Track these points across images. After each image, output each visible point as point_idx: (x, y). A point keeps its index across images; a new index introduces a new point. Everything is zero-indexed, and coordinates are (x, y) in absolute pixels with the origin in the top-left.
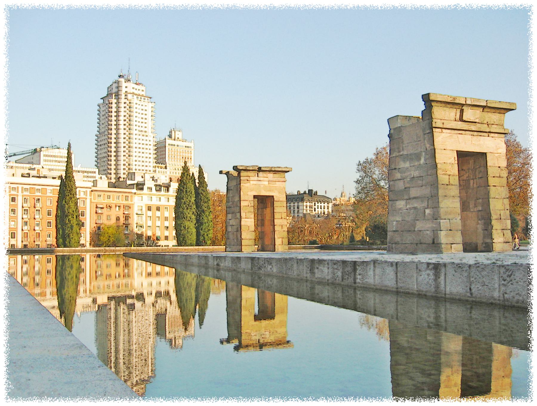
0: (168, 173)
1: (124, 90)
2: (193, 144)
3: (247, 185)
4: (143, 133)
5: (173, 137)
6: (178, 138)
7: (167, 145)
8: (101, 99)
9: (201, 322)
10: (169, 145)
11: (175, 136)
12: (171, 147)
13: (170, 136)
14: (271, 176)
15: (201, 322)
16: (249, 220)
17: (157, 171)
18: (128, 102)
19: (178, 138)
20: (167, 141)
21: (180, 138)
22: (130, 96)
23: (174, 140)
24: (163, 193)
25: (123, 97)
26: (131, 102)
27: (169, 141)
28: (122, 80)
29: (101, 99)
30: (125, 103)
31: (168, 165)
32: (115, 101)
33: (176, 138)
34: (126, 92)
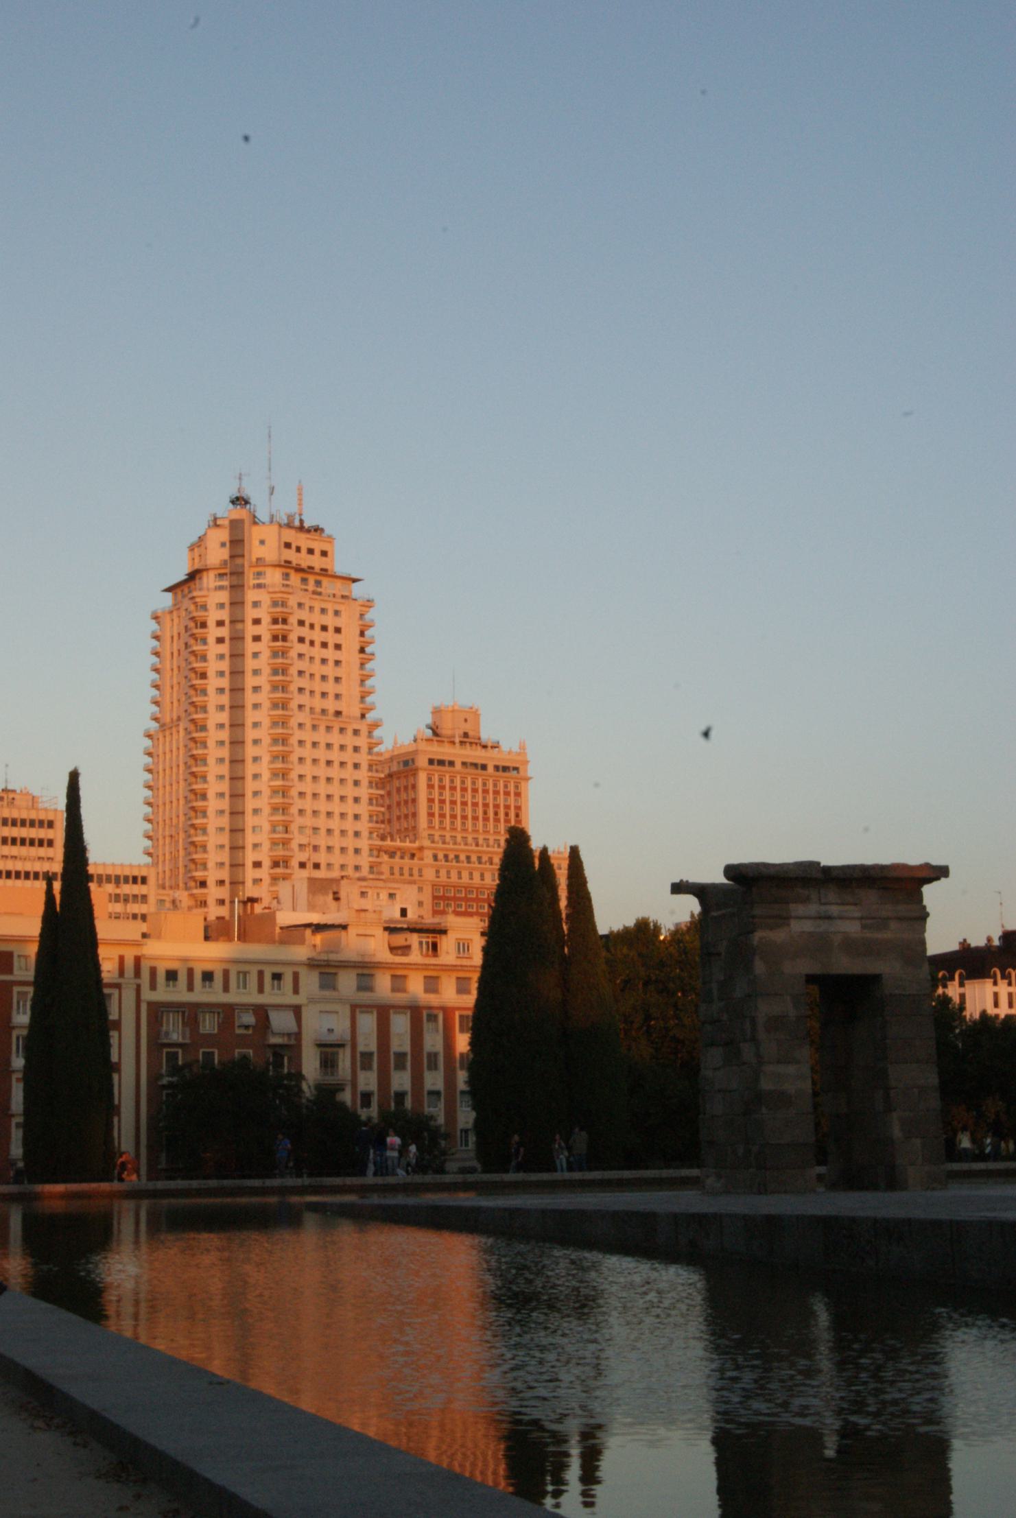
0: (429, 874)
3: (779, 936)
5: (446, 730)
6: (466, 735)
7: (422, 762)
10: (431, 762)
14: (870, 897)
16: (791, 1069)
17: (385, 869)
30: (256, 604)
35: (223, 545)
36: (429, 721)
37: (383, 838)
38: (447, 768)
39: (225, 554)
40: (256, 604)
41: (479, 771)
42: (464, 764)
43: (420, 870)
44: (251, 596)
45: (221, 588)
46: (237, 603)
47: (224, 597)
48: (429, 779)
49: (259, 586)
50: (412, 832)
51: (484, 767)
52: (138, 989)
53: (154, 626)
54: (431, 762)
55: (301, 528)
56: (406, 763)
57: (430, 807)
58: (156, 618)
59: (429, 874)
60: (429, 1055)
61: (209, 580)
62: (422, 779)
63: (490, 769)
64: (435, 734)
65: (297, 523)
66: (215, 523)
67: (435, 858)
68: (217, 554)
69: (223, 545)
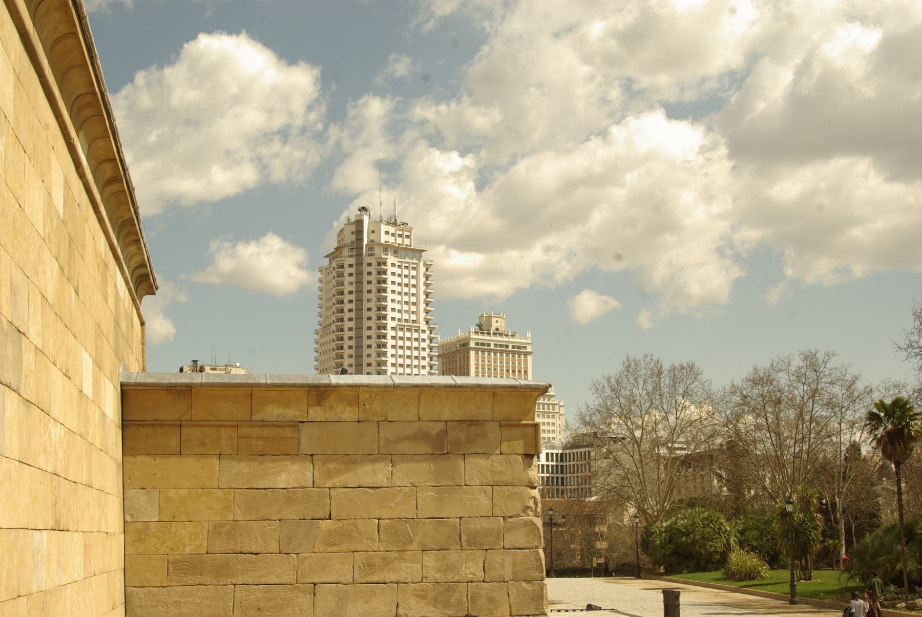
6: (497, 329)
7: (472, 344)
18: (374, 263)
19: (497, 329)
20: (473, 336)
21: (501, 330)
22: (378, 251)
23: (489, 334)
34: (372, 241)
35: (353, 233)
36: (478, 322)
39: (354, 237)
40: (369, 265)
44: (367, 260)
45: (351, 256)
46: (359, 264)
47: (352, 261)
49: (371, 255)
53: (319, 275)
54: (477, 344)
55: (395, 224)
56: (464, 345)
57: (477, 368)
58: (321, 271)
61: (346, 252)
62: (472, 353)
64: (481, 329)
65: (393, 221)
66: (349, 223)
68: (350, 238)
69: (353, 233)
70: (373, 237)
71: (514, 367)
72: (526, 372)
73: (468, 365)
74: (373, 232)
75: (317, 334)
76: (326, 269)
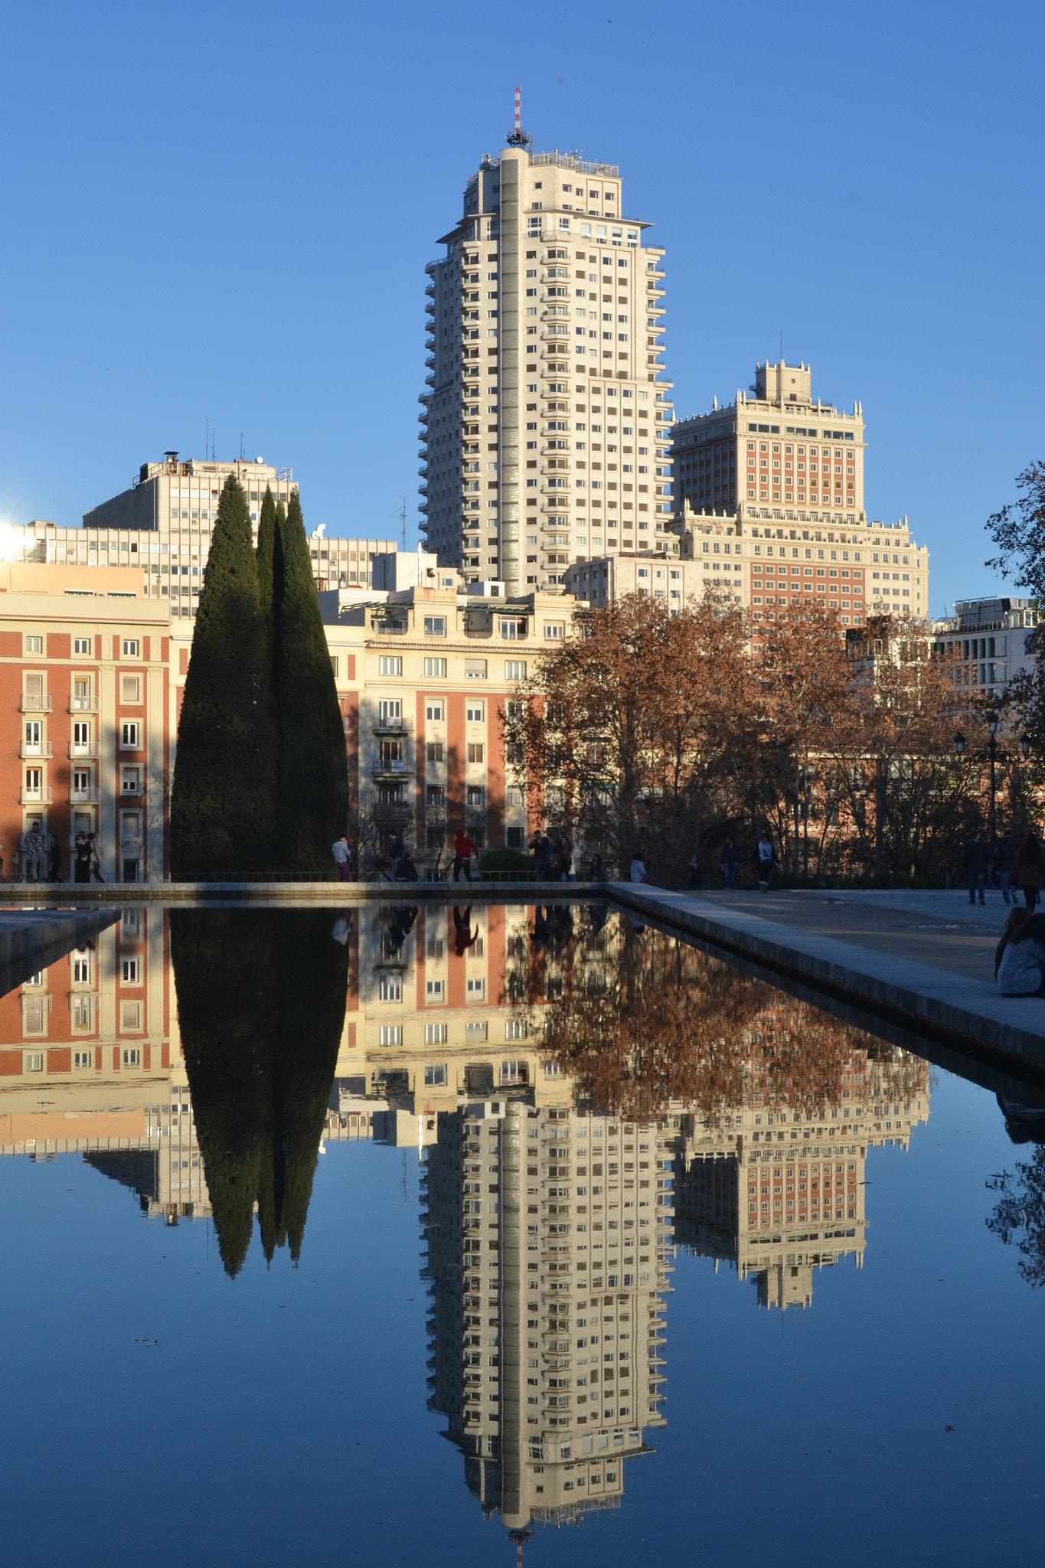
0: (748, 550)
1: (526, 196)
2: (859, 420)
4: (613, 383)
6: (793, 397)
7: (742, 427)
8: (439, 241)
9: (295, 1255)
10: (752, 427)
11: (779, 390)
12: (758, 437)
13: (760, 391)
15: (295, 1255)
18: (543, 251)
19: (793, 397)
20: (742, 410)
24: (496, 639)
25: (523, 226)
26: (560, 246)
27: (748, 414)
28: (518, 154)
29: (439, 241)
30: (531, 255)
31: (745, 516)
32: (492, 247)
33: (786, 394)
34: (536, 206)
37: (698, 512)
38: (770, 434)
41: (807, 438)
42: (790, 430)
43: (738, 547)
44: (523, 245)
48: (750, 447)
50: (729, 505)
51: (813, 433)
52: (166, 672)
53: (430, 282)
57: (751, 478)
58: (430, 270)
59: (748, 550)
60: (472, 746)
63: (820, 434)
67: (755, 533)
70: (538, 196)
71: (826, 476)
72: (850, 486)
73: (733, 471)
74: (538, 186)
75: (423, 400)
76: (442, 266)
